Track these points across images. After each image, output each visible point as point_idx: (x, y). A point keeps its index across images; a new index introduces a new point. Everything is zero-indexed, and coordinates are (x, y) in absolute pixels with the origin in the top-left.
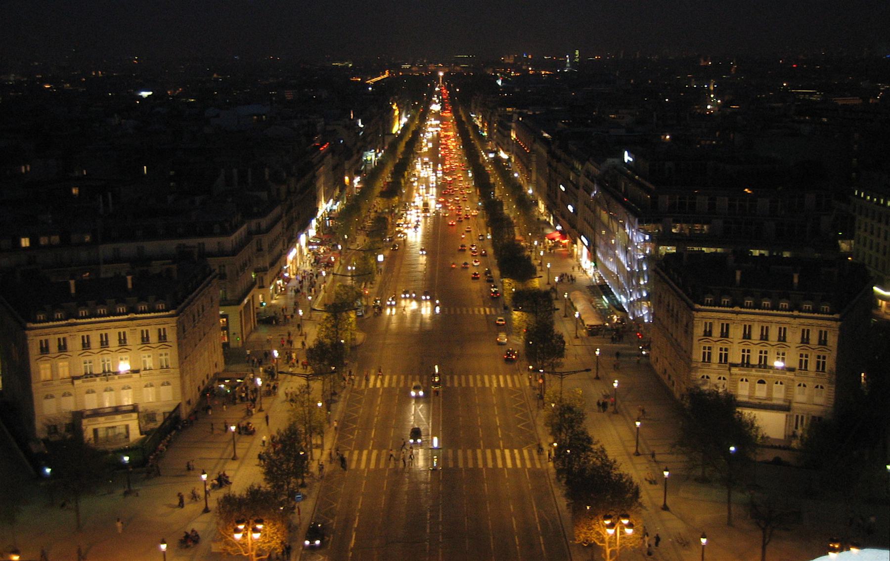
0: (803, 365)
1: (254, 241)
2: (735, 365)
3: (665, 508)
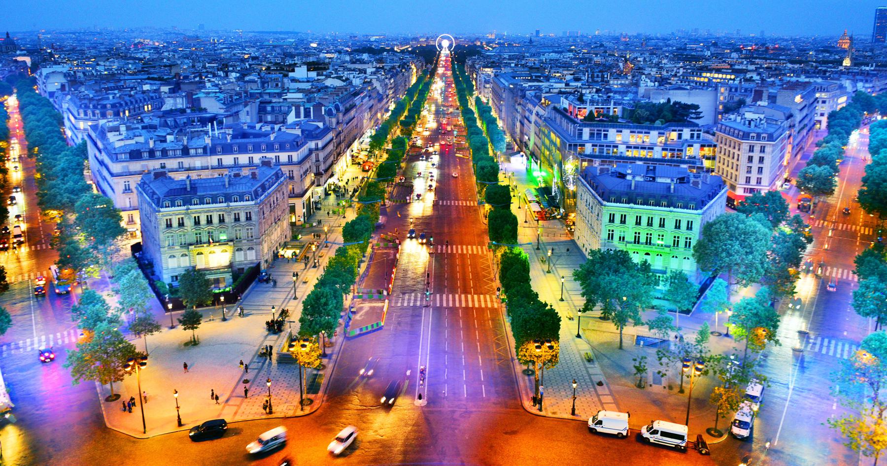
0: (676, 243)
1: (313, 155)
2: (630, 243)
3: (579, 336)
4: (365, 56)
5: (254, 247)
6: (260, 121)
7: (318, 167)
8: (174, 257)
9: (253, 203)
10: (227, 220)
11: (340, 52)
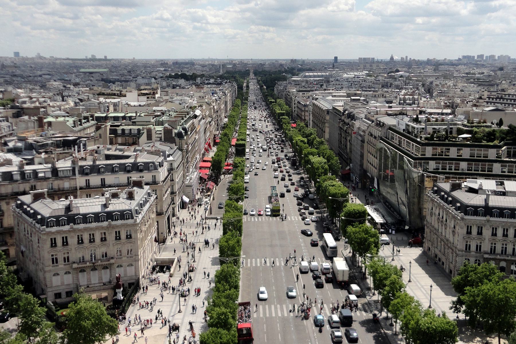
4: (182, 82)
5: (134, 263)
6: (111, 143)
7: (172, 186)
8: (58, 274)
9: (130, 221)
10: (108, 239)
11: (155, 79)
